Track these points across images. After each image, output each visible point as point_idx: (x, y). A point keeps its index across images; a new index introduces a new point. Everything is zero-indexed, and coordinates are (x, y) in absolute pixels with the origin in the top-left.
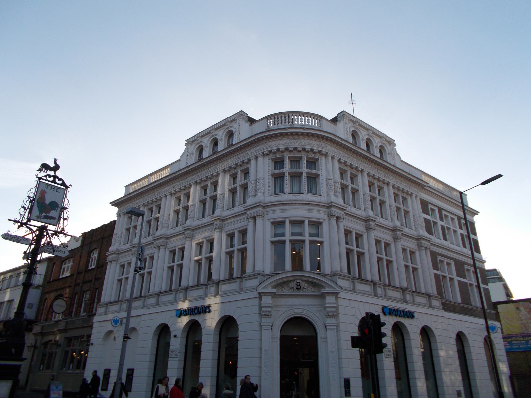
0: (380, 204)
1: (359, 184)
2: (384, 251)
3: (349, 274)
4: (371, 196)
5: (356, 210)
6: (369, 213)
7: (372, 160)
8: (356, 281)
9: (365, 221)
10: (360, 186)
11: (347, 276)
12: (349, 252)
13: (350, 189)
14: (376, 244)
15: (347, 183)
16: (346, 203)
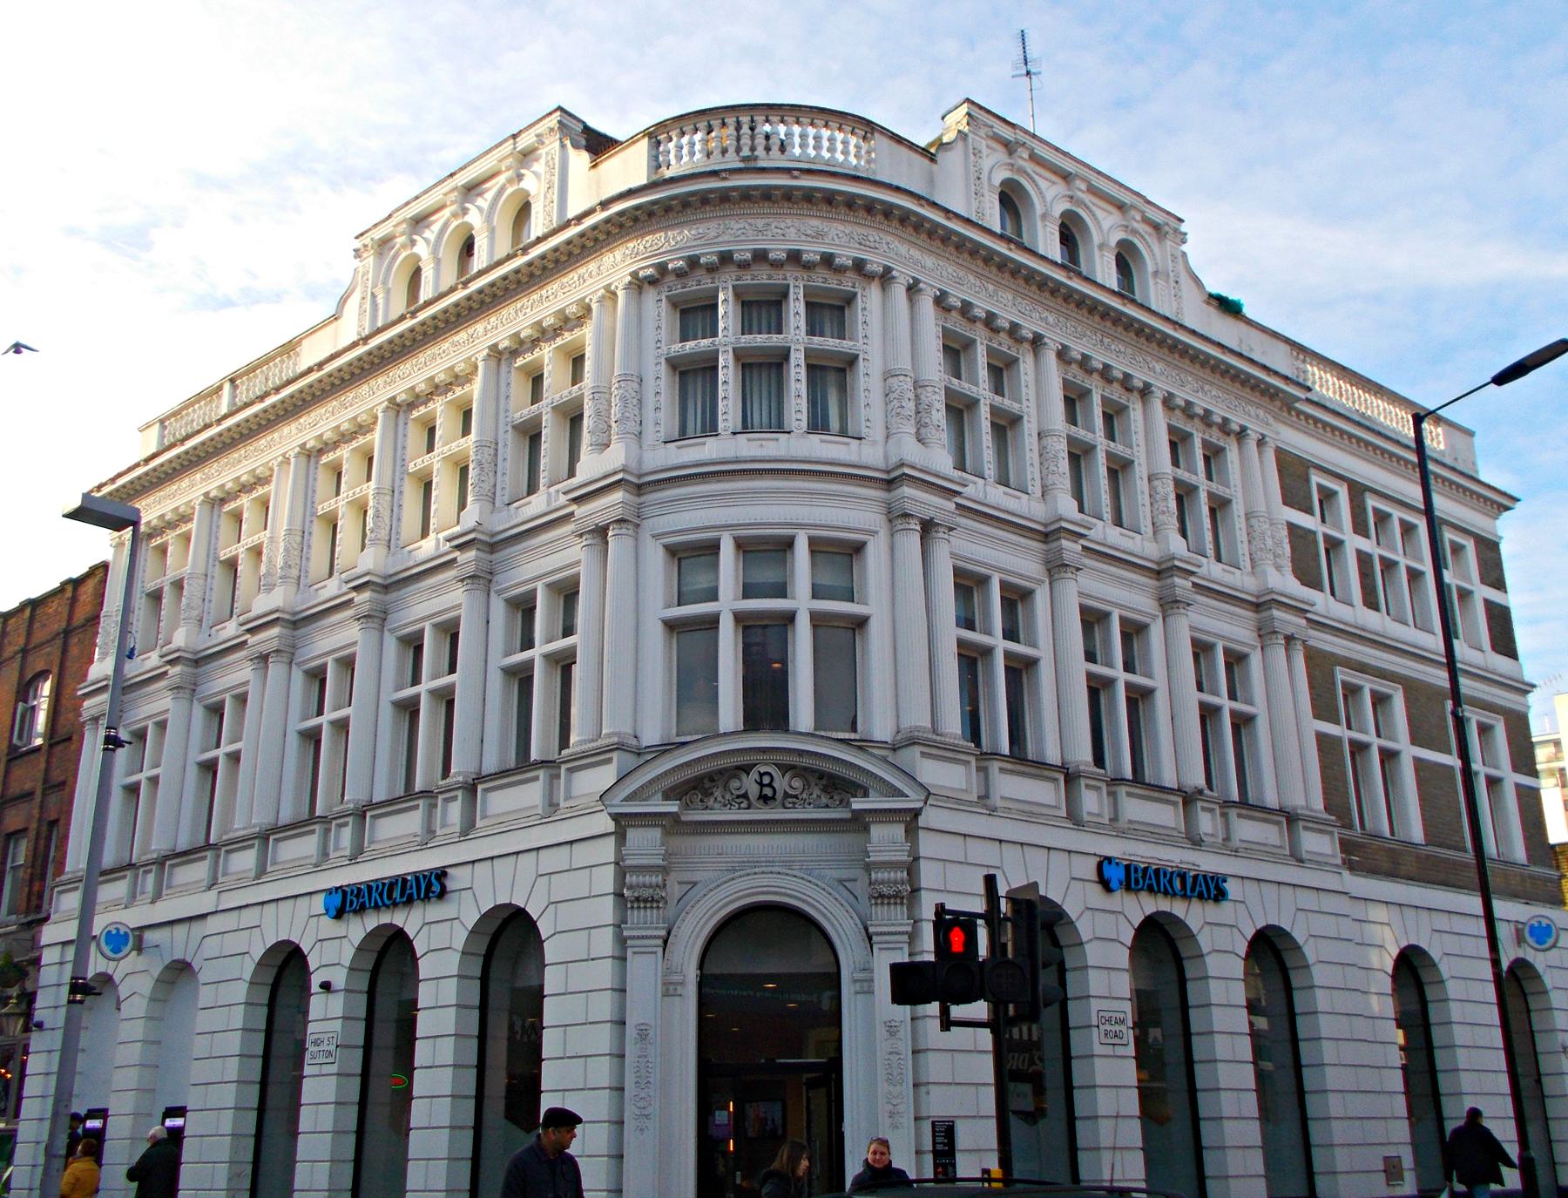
0: (1213, 511)
1: (1134, 439)
2: (1225, 679)
3: (1098, 767)
4: (1178, 483)
5: (1226, 571)
6: (1171, 548)
7: (1169, 341)
8: (1122, 790)
9: (1254, 609)
10: (1138, 445)
11: (1326, 820)
12: (1099, 687)
13: (1203, 496)
14: (1196, 656)
15: (1227, 490)
16: (1086, 510)
